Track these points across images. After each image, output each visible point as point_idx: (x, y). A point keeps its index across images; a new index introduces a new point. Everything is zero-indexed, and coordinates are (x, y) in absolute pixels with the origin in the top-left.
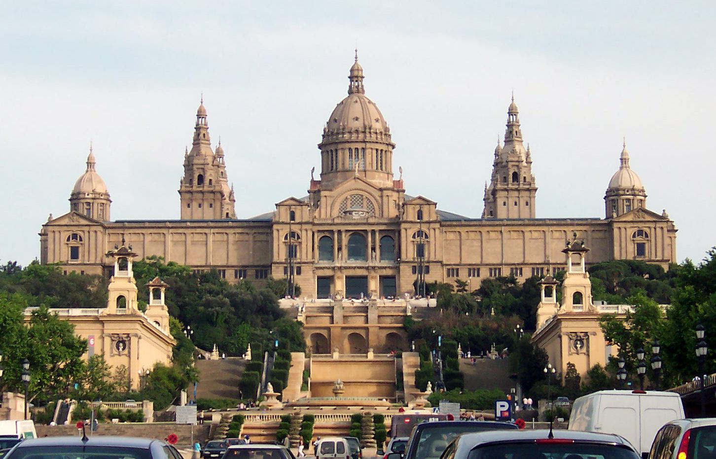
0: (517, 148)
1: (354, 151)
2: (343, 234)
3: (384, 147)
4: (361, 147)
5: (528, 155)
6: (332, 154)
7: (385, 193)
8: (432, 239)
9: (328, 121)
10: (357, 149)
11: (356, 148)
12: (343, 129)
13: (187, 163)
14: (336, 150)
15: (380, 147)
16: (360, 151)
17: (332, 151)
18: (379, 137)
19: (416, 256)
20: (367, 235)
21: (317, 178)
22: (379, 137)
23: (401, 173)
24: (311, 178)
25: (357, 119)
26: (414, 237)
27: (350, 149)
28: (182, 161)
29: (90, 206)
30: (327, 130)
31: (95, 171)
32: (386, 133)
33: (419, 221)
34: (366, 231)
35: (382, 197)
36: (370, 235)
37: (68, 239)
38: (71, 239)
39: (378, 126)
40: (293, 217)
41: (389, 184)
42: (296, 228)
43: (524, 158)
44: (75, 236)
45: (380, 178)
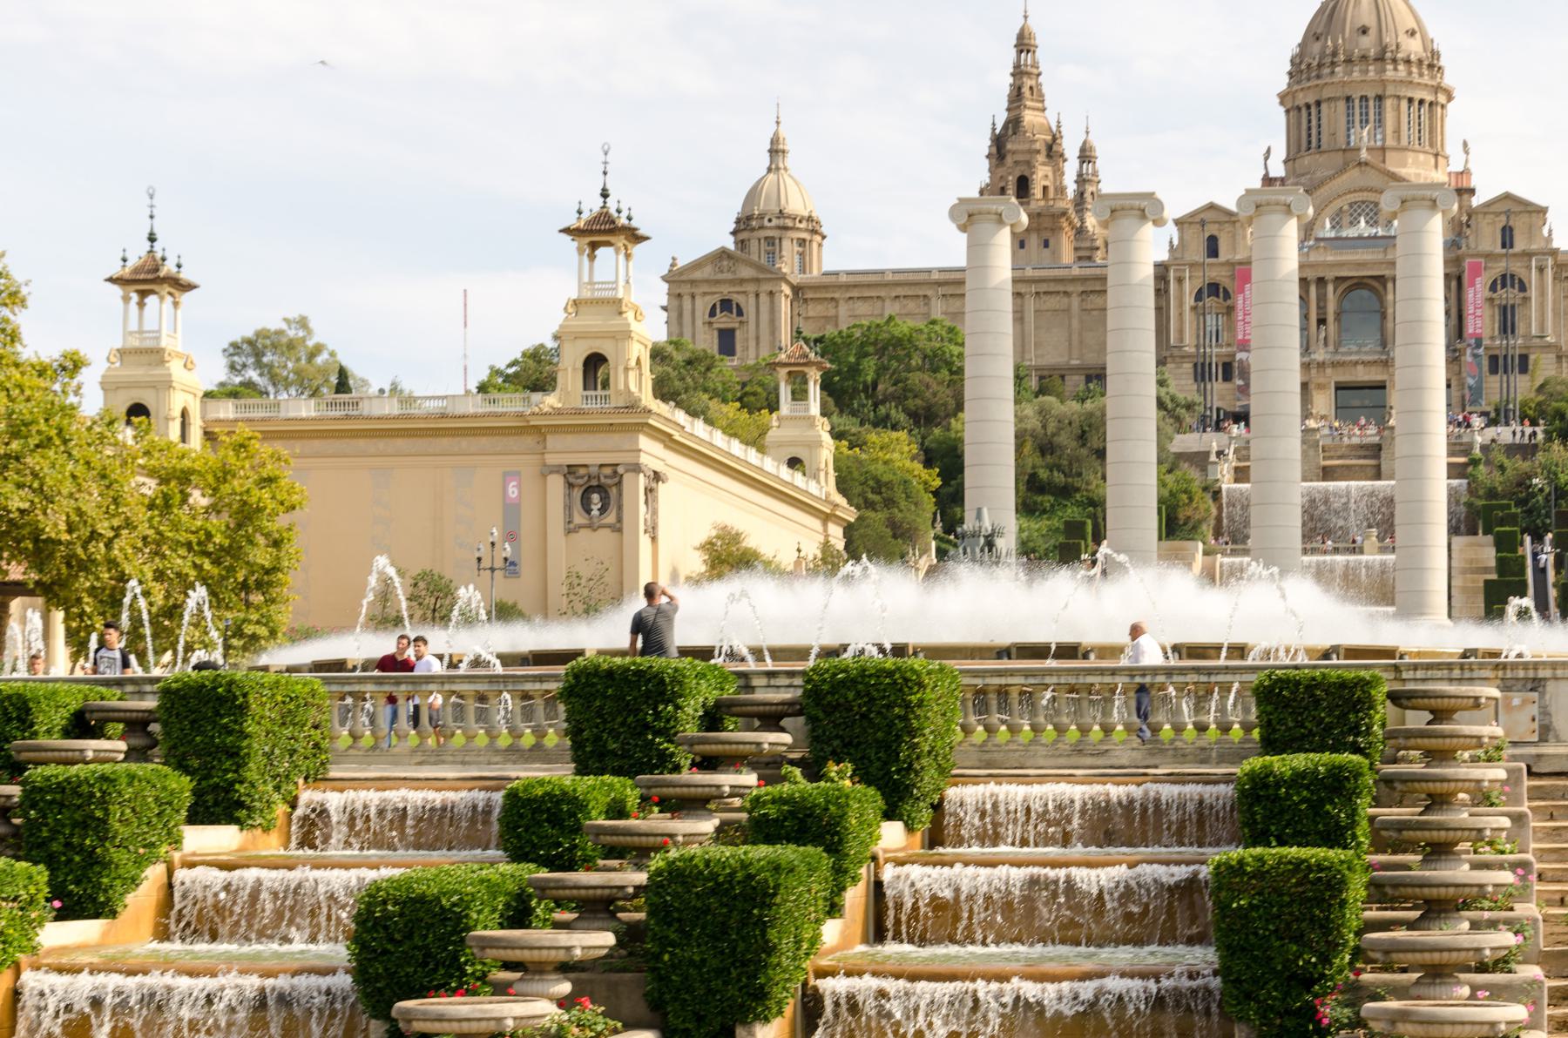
1: (1357, 102)
2: (1330, 288)
3: (1429, 98)
4: (1373, 95)
6: (1310, 114)
8: (1533, 293)
9: (1299, 40)
10: (1364, 98)
11: (1362, 97)
12: (1335, 54)
13: (994, 150)
14: (1318, 103)
15: (1418, 95)
16: (1371, 103)
17: (1308, 106)
18: (1415, 70)
19: (1497, 333)
20: (1385, 287)
21: (1277, 170)
22: (1415, 70)
23: (1467, 153)
24: (1264, 172)
25: (1364, 31)
26: (1493, 288)
27: (1348, 99)
28: (984, 144)
29: (773, 244)
30: (1298, 61)
31: (786, 169)
32: (1432, 63)
33: (1504, 251)
37: (712, 313)
38: (718, 310)
39: (1413, 47)
40: (1213, 251)
41: (1440, 176)
42: (1217, 274)
44: (726, 304)
45: (1416, 163)
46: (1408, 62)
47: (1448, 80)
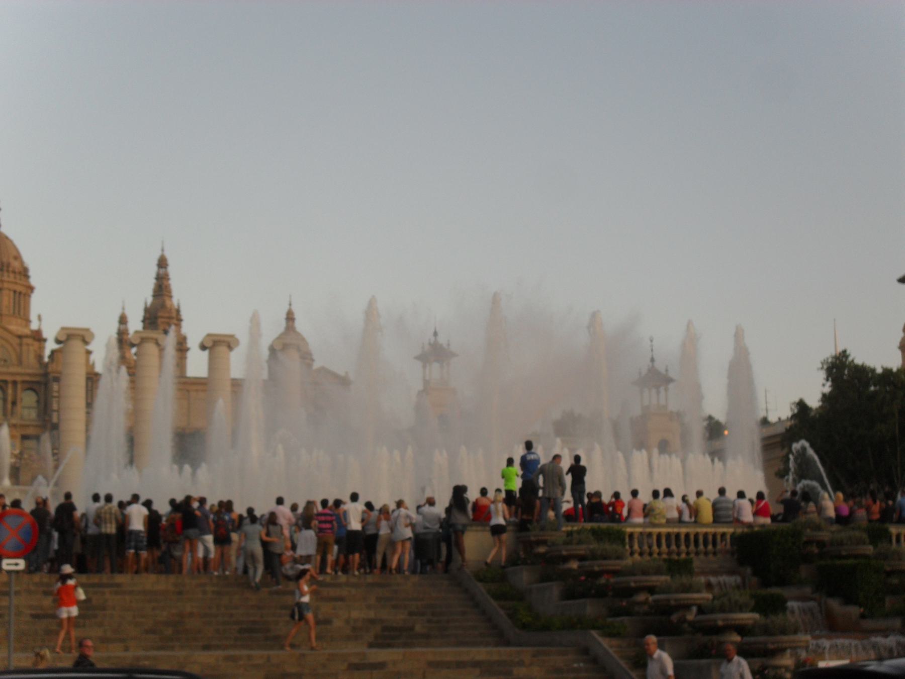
0: (168, 303)
5: (178, 311)
7: (25, 340)
34: (6, 382)
35: (21, 345)
36: (10, 387)
39: (16, 264)
41: (26, 331)
43: (174, 315)
46: (14, 272)
47: (33, 281)
